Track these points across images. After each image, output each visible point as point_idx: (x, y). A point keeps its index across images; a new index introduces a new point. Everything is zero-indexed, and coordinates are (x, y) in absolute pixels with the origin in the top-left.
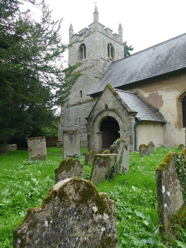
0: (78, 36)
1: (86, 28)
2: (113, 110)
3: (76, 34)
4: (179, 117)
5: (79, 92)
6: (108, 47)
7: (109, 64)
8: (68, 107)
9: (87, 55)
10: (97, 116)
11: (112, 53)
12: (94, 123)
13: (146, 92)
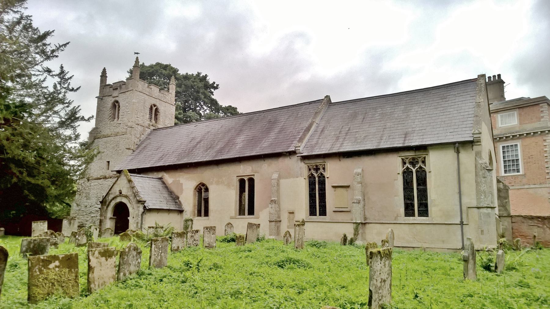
0: (111, 89)
1: (122, 81)
2: (126, 197)
3: (109, 85)
6: (151, 109)
7: (148, 131)
8: (88, 180)
9: (120, 116)
10: (111, 201)
11: (156, 115)
12: (107, 207)
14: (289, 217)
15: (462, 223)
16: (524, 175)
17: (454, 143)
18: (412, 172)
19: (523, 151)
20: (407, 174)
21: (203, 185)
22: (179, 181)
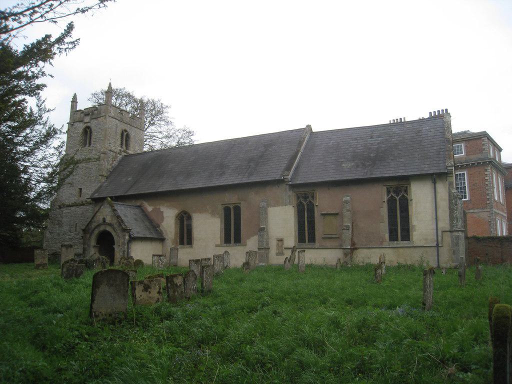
0: (83, 115)
2: (110, 225)
3: (80, 110)
4: (176, 234)
5: (78, 190)
7: (120, 157)
9: (92, 143)
10: (94, 229)
11: (127, 141)
12: (91, 235)
13: (150, 206)
14: (278, 244)
15: (437, 246)
16: (470, 201)
17: (432, 175)
18: (396, 200)
19: (469, 179)
20: (391, 202)
21: (185, 213)
22: (159, 209)
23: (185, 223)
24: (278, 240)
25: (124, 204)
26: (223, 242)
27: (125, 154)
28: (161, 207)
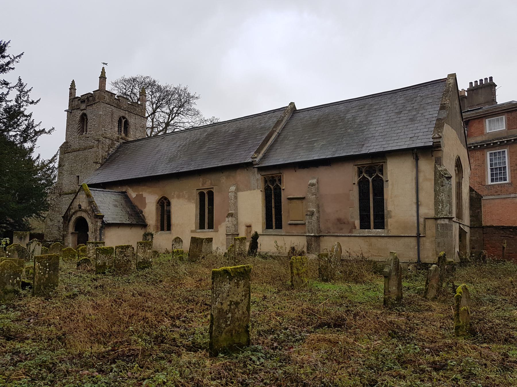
0: (79, 102)
1: (90, 93)
2: (85, 211)
3: (78, 97)
4: (157, 220)
5: (76, 178)
6: (120, 121)
7: (117, 144)
8: (60, 195)
9: (88, 130)
12: (69, 222)
13: (134, 192)
14: (247, 230)
15: (418, 237)
16: (510, 184)
17: (412, 149)
18: (368, 181)
19: (510, 158)
20: (363, 185)
21: (166, 198)
22: (142, 195)
23: (165, 208)
24: (247, 226)
25: (97, 189)
26: (199, 228)
27: (124, 141)
28: (143, 193)
